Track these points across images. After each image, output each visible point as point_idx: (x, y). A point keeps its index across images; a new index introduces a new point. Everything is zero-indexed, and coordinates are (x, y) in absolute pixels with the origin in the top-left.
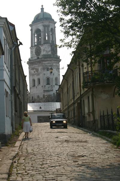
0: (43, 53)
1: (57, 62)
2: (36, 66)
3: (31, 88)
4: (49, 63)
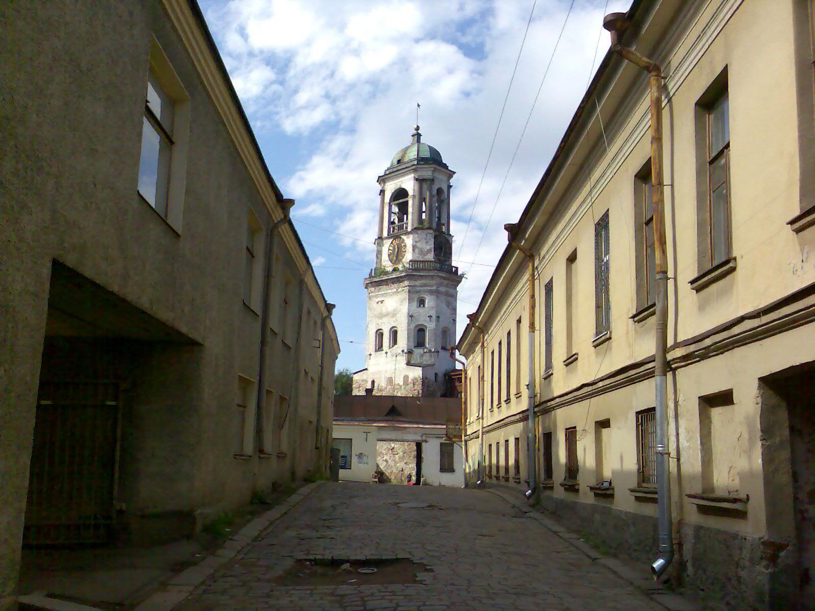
1: (450, 283)
3: (370, 355)
4: (425, 285)
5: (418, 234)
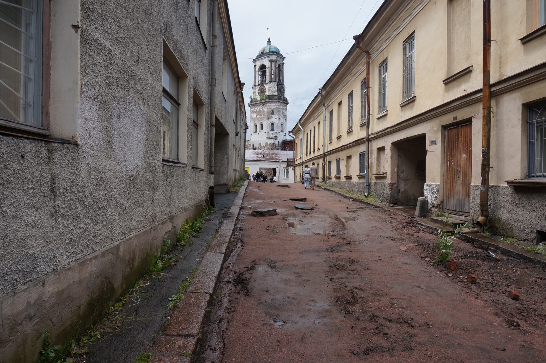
0: (267, 93)
2: (259, 108)
4: (274, 106)
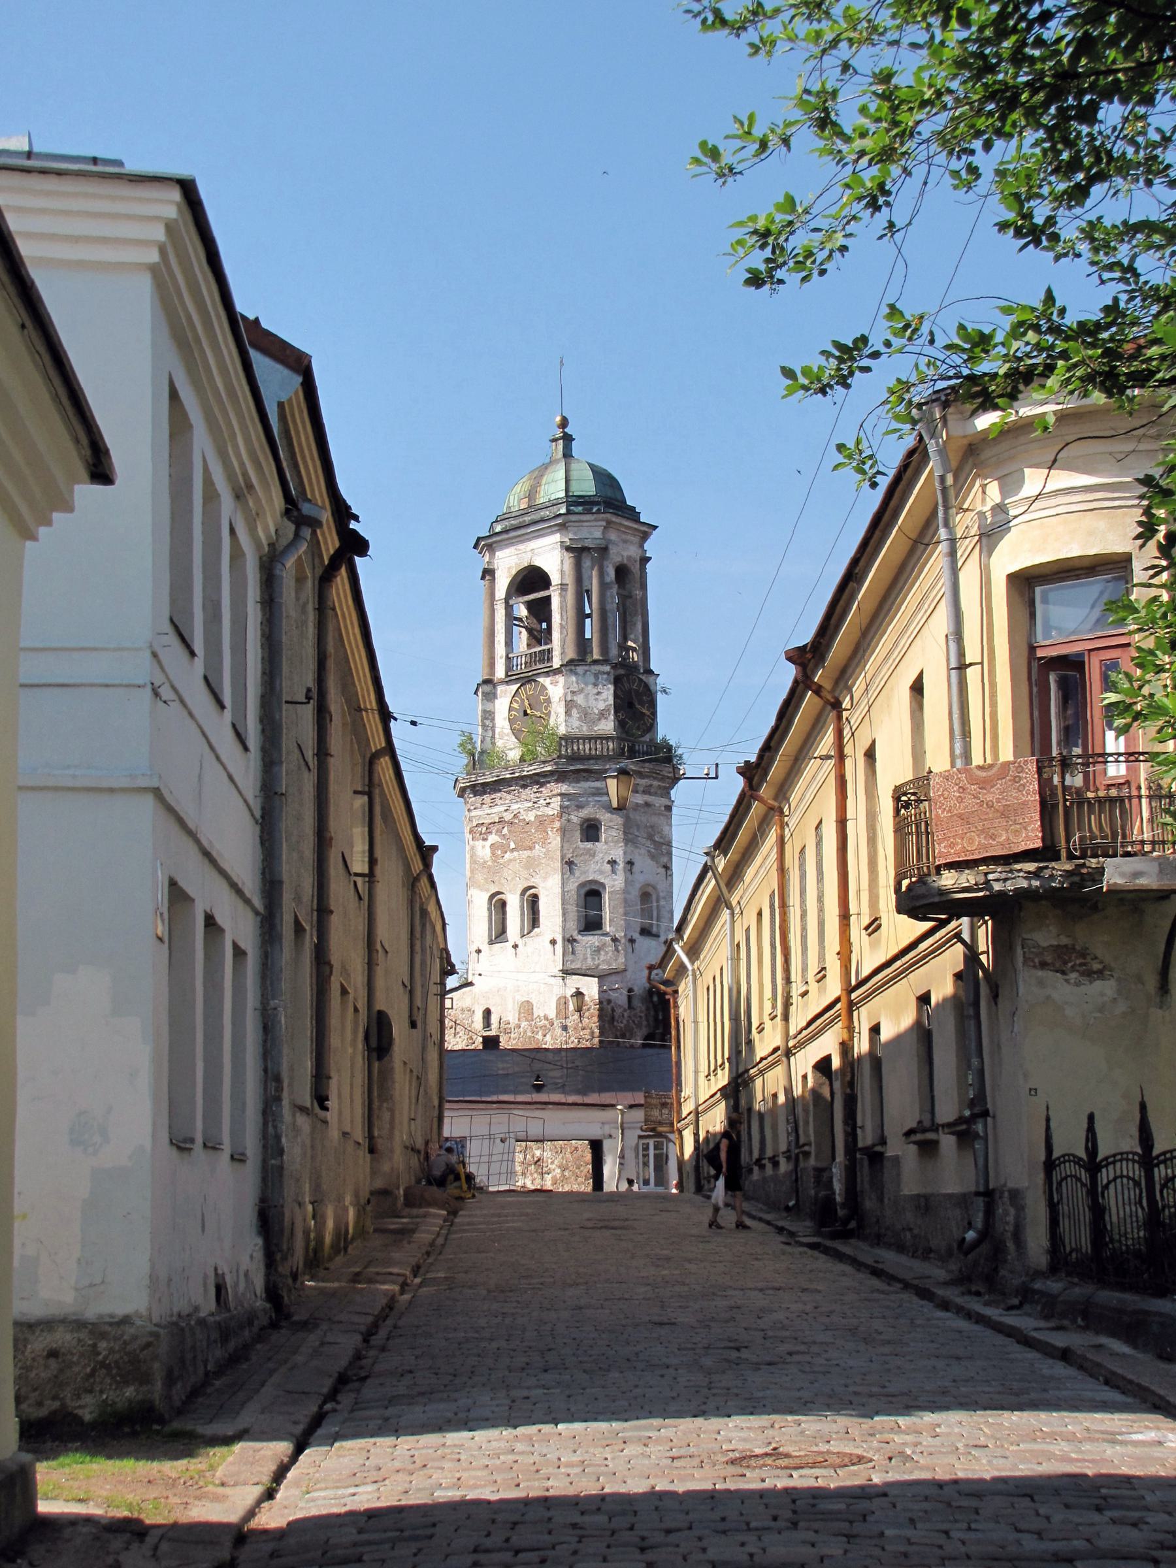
1: (656, 783)
3: (479, 951)
5: (576, 674)
